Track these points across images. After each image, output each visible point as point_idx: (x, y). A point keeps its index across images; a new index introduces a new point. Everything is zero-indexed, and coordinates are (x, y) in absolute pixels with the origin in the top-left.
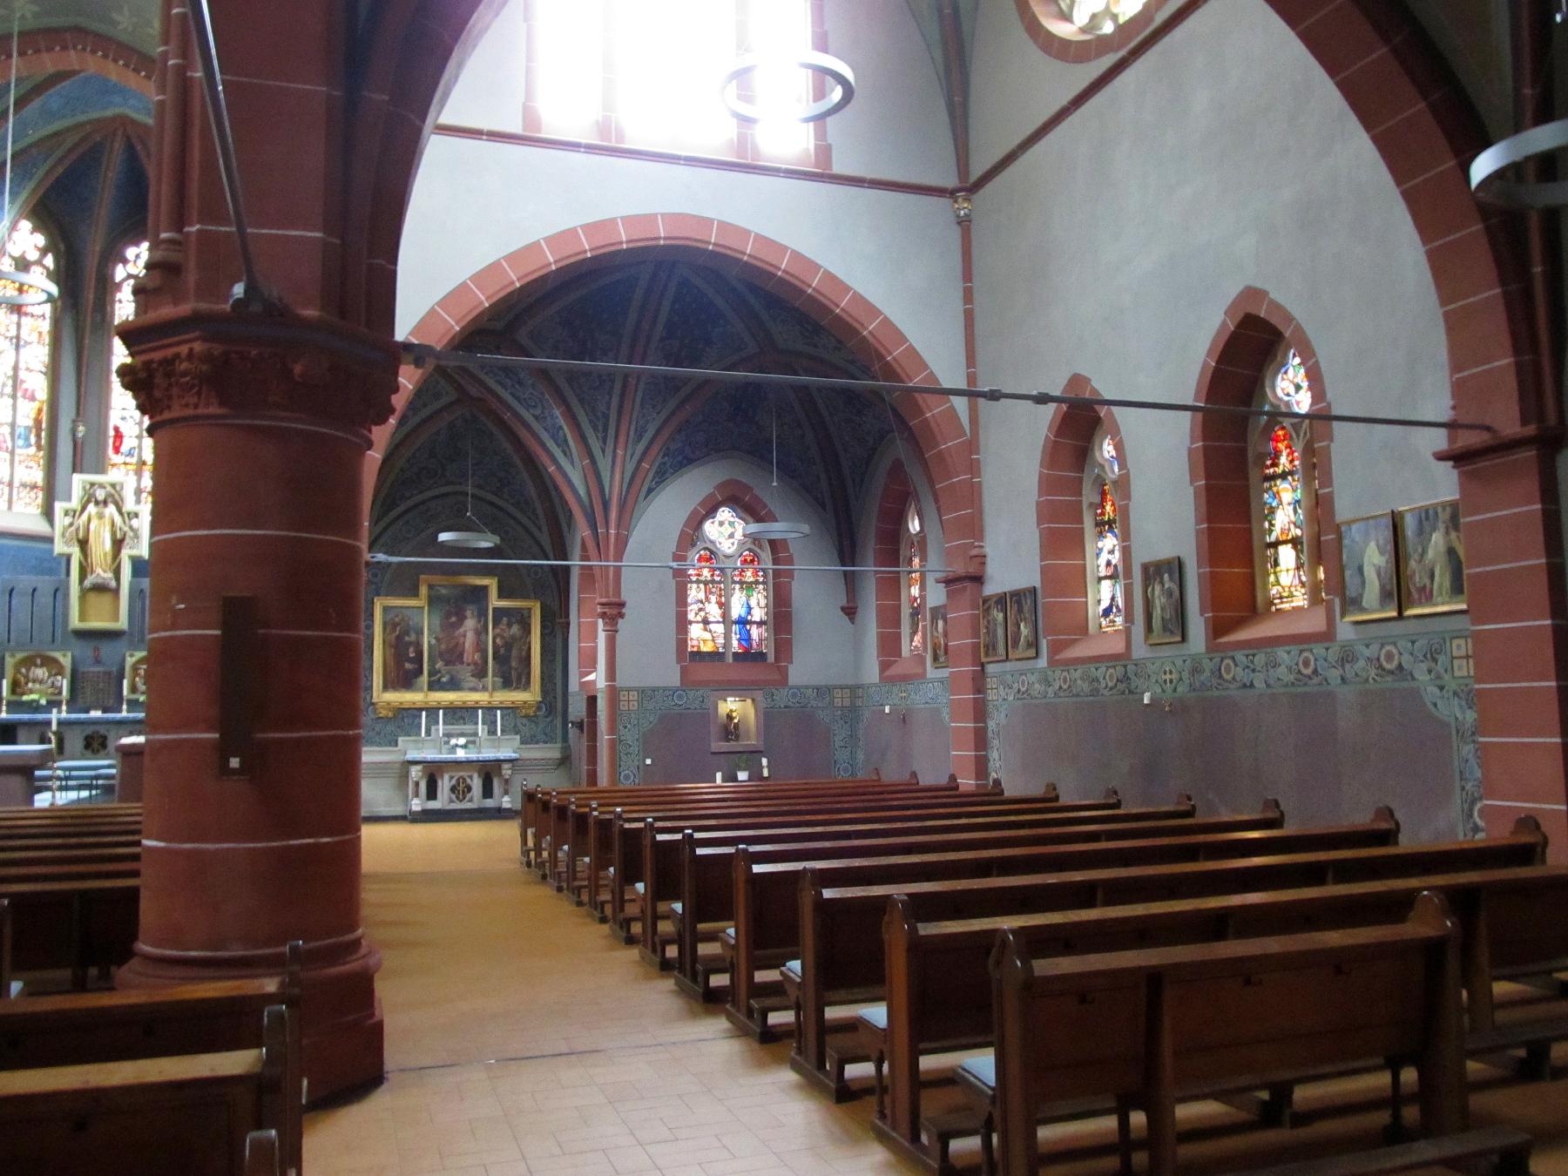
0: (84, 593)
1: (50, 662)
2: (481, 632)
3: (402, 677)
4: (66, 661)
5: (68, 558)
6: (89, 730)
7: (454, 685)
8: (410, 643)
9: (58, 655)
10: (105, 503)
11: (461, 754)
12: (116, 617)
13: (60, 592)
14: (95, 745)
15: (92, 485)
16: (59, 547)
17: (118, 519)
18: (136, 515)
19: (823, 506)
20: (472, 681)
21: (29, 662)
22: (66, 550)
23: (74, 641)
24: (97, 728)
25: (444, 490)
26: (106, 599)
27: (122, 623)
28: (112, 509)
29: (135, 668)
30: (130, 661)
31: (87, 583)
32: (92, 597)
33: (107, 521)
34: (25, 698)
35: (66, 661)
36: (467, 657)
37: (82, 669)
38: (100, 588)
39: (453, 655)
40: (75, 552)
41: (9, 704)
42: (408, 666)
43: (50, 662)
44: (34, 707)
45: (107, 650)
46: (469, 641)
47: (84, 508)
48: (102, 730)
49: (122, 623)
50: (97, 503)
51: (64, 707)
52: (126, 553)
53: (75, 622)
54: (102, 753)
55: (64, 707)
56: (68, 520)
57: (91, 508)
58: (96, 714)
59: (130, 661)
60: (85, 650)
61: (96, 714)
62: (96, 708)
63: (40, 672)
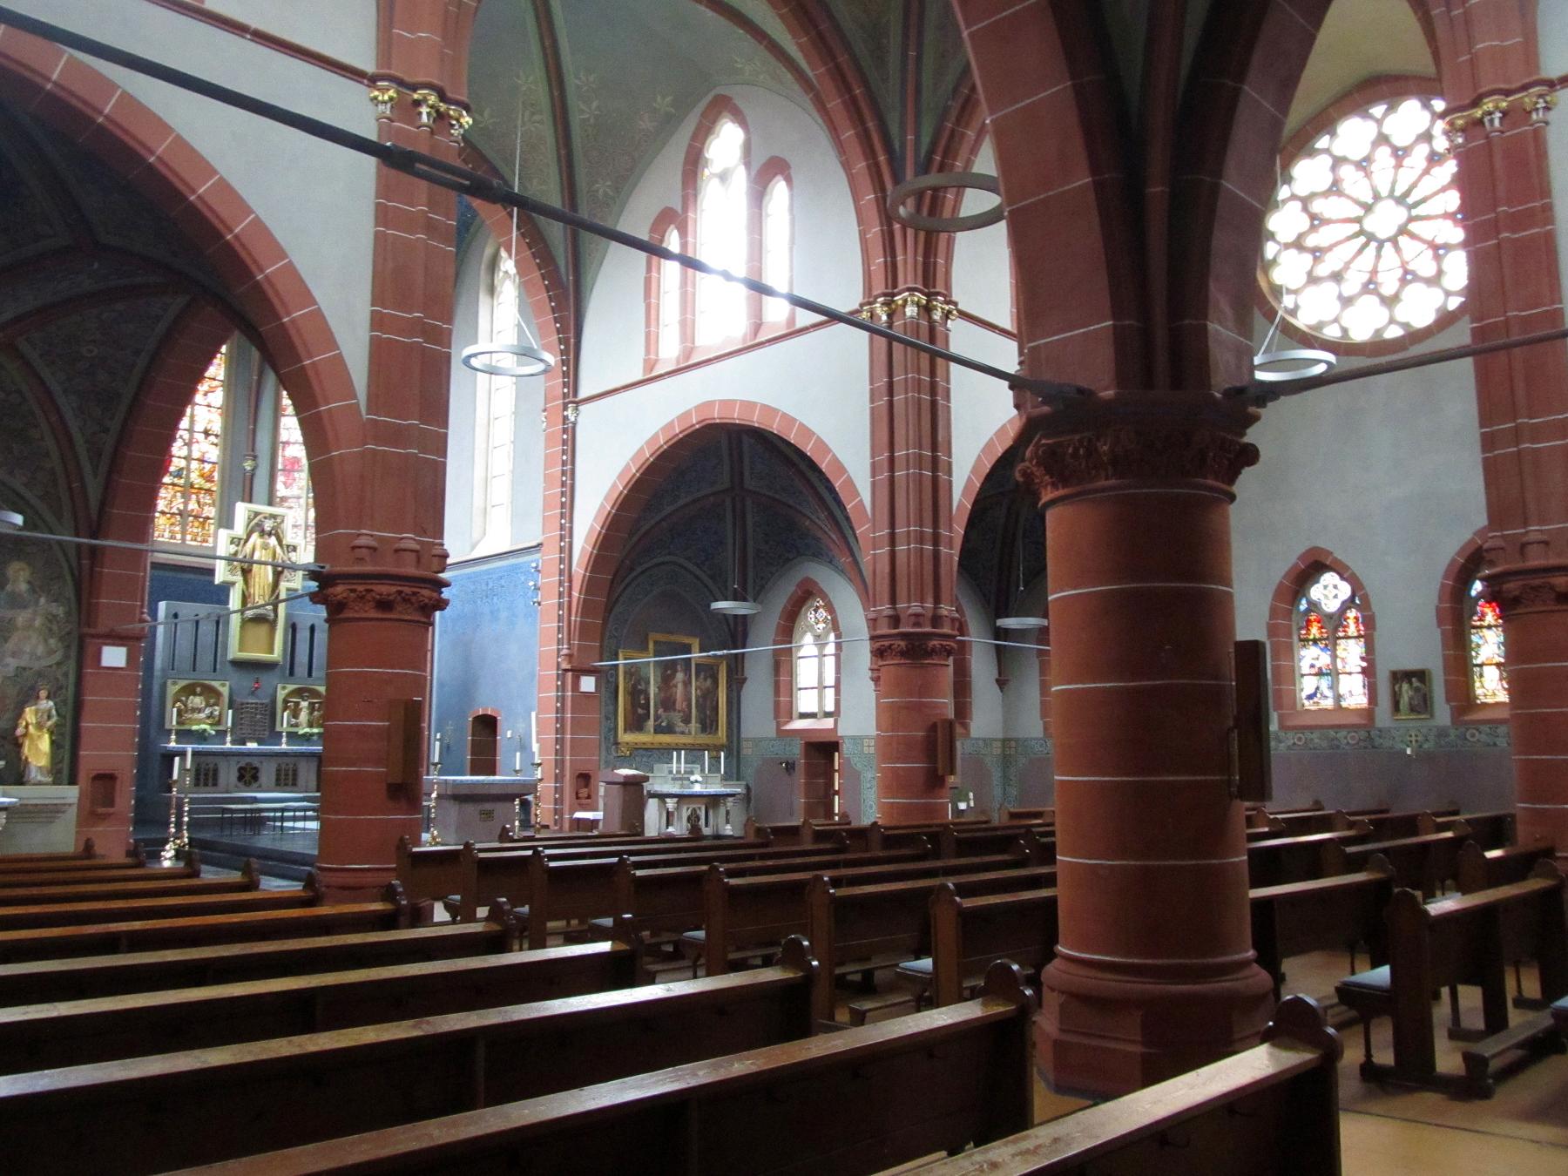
0: (245, 622)
1: (211, 693)
2: (687, 684)
3: (636, 724)
4: (225, 691)
5: (226, 588)
6: (244, 762)
7: (669, 730)
8: (641, 692)
9: (216, 684)
10: (270, 534)
11: (697, 789)
12: (271, 651)
13: (220, 622)
14: (247, 777)
15: (257, 514)
16: (221, 574)
17: (278, 550)
18: (295, 549)
19: (988, 602)
20: (680, 726)
21: (190, 690)
22: (230, 578)
23: (229, 668)
24: (248, 760)
25: (668, 558)
26: (263, 630)
27: (277, 654)
28: (273, 541)
29: (285, 701)
30: (281, 694)
31: (249, 613)
32: (250, 626)
33: (270, 552)
34: (195, 728)
35: (225, 691)
36: (678, 706)
37: (239, 700)
38: (259, 619)
39: (667, 703)
40: (239, 579)
41: (178, 733)
42: (640, 711)
43: (211, 693)
44: (201, 737)
45: (267, 679)
46: (680, 690)
47: (249, 536)
48: (255, 762)
49: (277, 654)
50: (263, 533)
51: (229, 739)
52: (283, 585)
53: (234, 652)
54: (255, 785)
55: (229, 739)
56: (233, 549)
57: (255, 536)
58: (252, 746)
59: (281, 694)
60: (246, 681)
61: (252, 746)
62: (252, 740)
63: (197, 701)
